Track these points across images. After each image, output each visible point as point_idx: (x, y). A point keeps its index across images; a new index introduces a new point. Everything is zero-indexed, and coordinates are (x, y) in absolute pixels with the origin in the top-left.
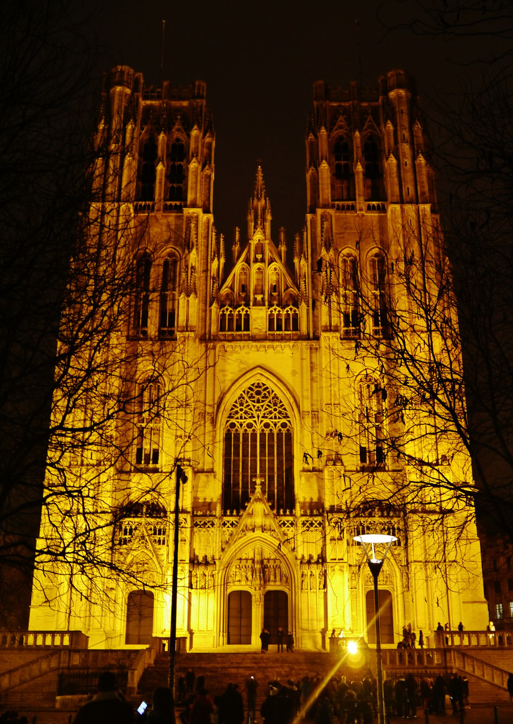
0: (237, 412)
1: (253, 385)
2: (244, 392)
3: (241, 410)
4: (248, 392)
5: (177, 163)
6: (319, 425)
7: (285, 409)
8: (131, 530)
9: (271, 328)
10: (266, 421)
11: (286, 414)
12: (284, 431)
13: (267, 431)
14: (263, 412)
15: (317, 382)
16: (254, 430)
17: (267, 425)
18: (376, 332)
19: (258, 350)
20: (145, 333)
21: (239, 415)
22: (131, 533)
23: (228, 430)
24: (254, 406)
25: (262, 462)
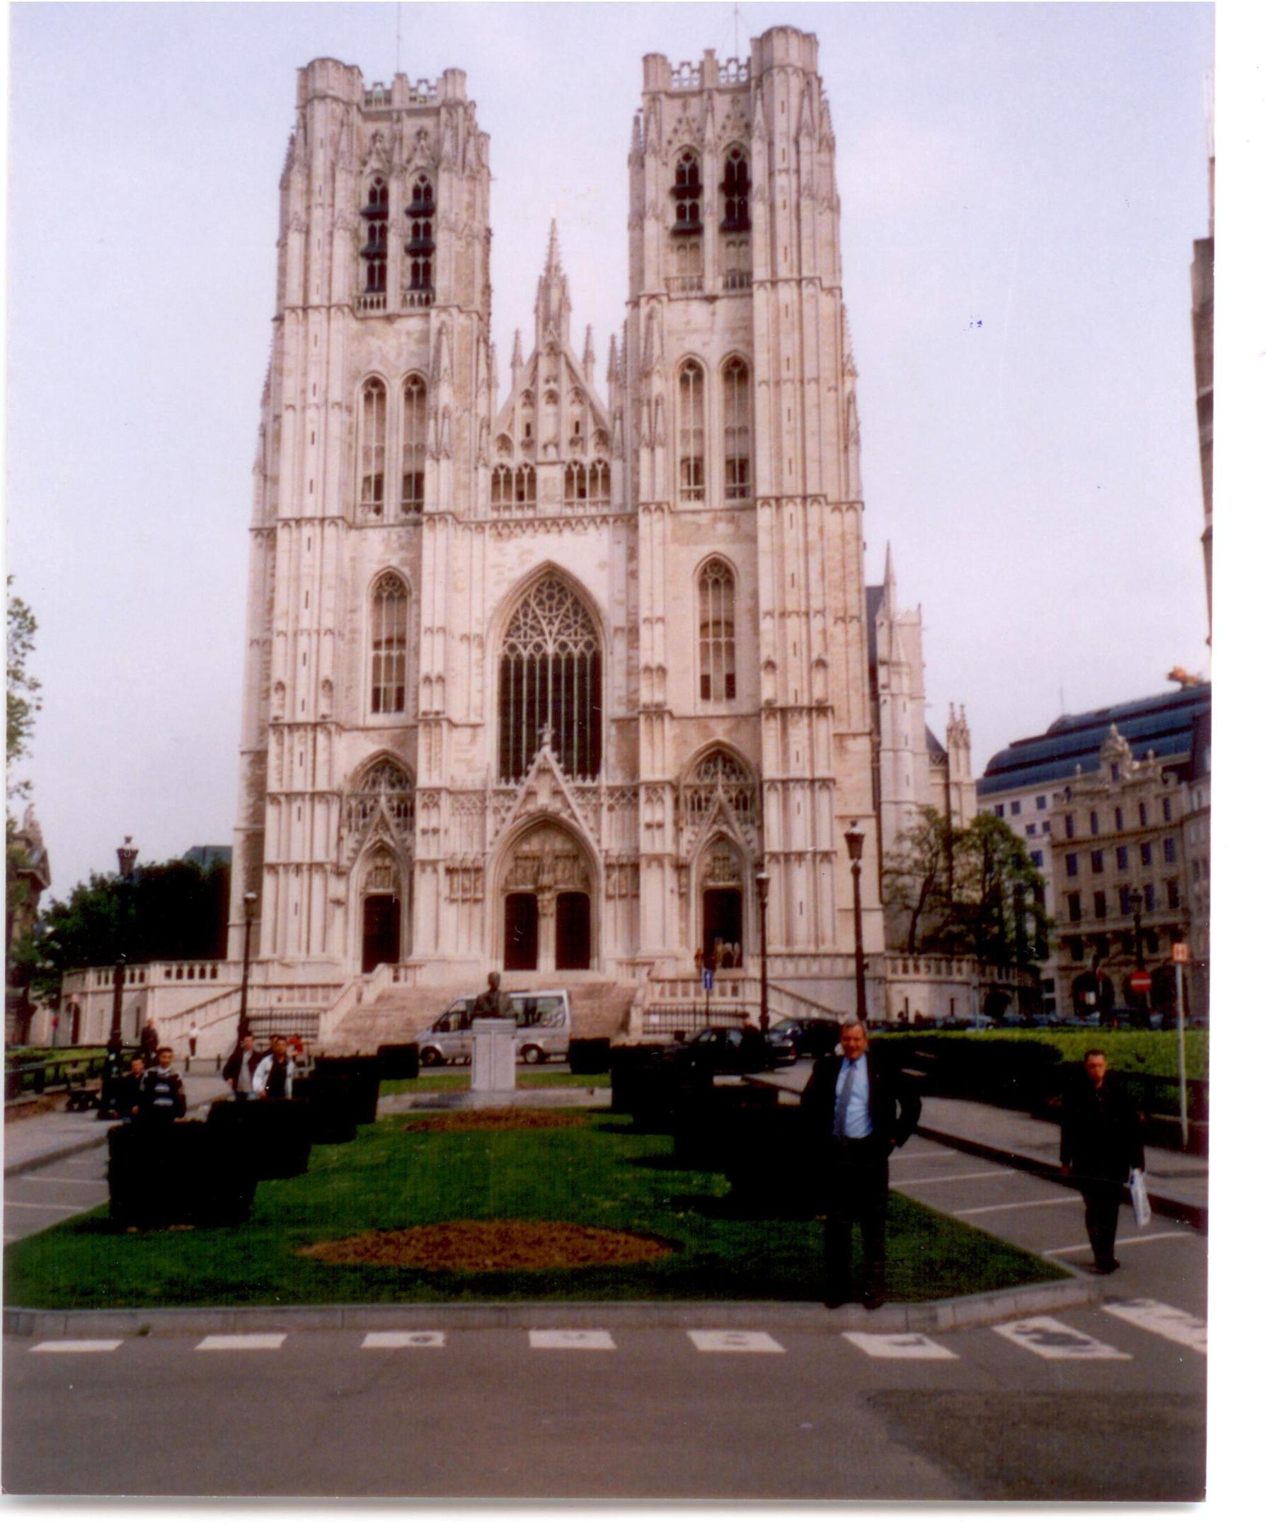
0: (518, 628)
1: (543, 584)
3: (525, 624)
4: (535, 597)
5: (422, 221)
7: (590, 621)
9: (568, 492)
10: (562, 638)
12: (589, 655)
13: (563, 657)
17: (563, 646)
18: (730, 494)
19: (548, 531)
20: (378, 510)
21: (522, 633)
22: (365, 815)
24: (544, 617)
25: (556, 702)
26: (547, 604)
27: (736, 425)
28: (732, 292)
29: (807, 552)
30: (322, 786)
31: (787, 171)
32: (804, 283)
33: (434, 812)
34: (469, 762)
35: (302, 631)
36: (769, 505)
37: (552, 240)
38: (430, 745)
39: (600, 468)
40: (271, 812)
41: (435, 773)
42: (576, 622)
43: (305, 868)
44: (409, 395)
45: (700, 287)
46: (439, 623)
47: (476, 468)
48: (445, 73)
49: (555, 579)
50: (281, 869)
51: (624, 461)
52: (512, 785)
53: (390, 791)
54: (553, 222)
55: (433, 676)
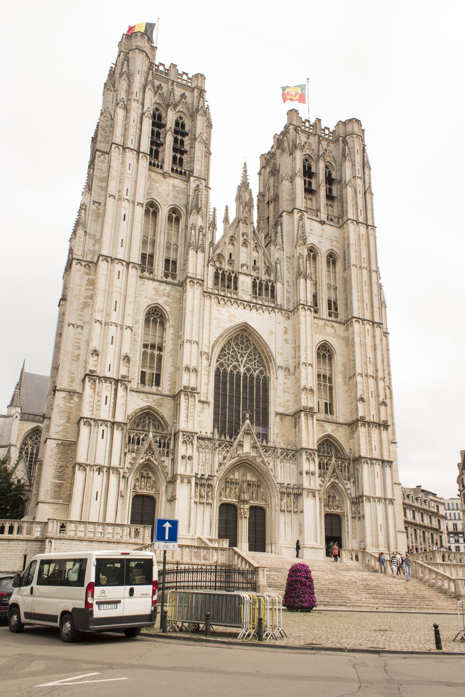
0: (225, 355)
1: (238, 335)
2: (231, 339)
3: (229, 354)
6: (291, 377)
7: (262, 360)
8: (138, 440)
11: (263, 364)
14: (245, 359)
15: (288, 343)
16: (238, 372)
17: (248, 370)
18: (330, 315)
19: (245, 308)
20: (151, 272)
21: (227, 357)
22: (138, 443)
23: (218, 368)
24: (239, 353)
25: (245, 399)
26: (241, 346)
27: (332, 283)
28: (331, 223)
29: (375, 350)
30: (120, 418)
31: (360, 178)
32: (370, 227)
33: (189, 446)
34: (200, 422)
35: (112, 324)
36: (359, 323)
37: (245, 171)
38: (188, 407)
39: (270, 284)
40: (84, 430)
41: (190, 423)
42: (255, 359)
43: (105, 469)
44: (170, 218)
45: (317, 216)
46: (195, 339)
47: (208, 266)
48: (196, 76)
49: (245, 334)
50: (88, 468)
51: (283, 284)
52: (228, 438)
53: (155, 431)
54: (245, 164)
55: (191, 367)
